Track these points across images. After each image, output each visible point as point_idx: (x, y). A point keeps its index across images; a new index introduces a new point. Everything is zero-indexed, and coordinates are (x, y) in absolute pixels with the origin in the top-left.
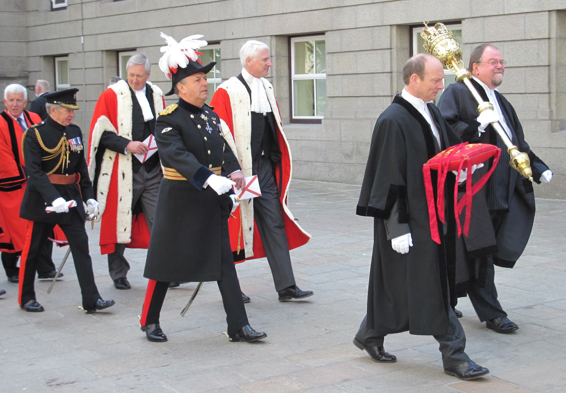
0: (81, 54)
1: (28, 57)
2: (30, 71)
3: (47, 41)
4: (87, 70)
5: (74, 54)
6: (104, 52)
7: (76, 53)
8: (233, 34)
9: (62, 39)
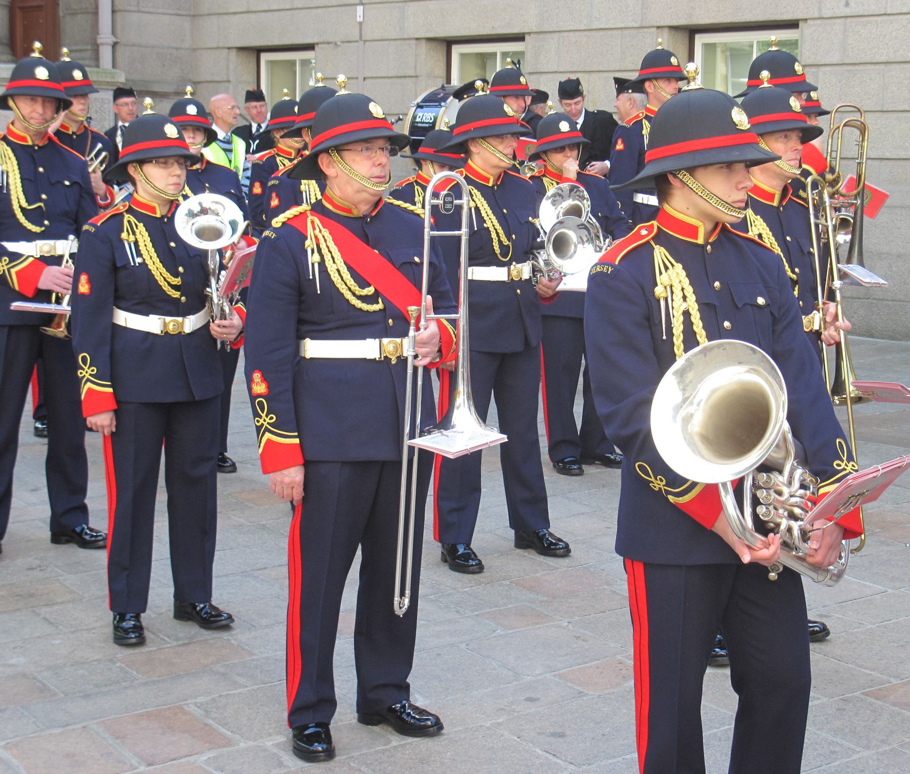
0: (355, 44)
1: (194, 50)
2: (198, 80)
3: (253, 16)
4: (367, 81)
5: (336, 44)
6: (424, 41)
7: (339, 43)
8: (847, 4)
9: (298, 11)
